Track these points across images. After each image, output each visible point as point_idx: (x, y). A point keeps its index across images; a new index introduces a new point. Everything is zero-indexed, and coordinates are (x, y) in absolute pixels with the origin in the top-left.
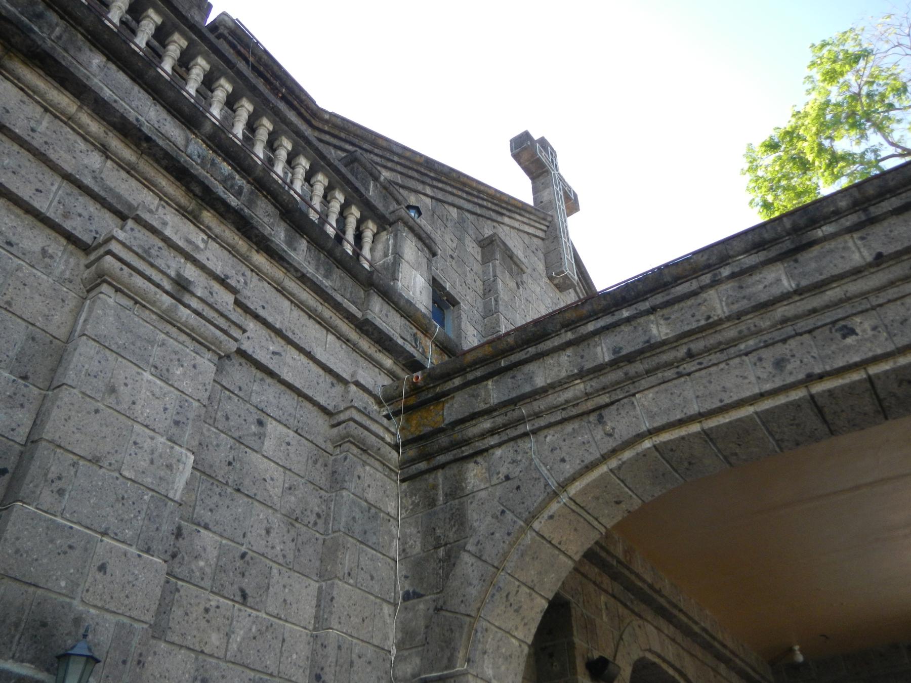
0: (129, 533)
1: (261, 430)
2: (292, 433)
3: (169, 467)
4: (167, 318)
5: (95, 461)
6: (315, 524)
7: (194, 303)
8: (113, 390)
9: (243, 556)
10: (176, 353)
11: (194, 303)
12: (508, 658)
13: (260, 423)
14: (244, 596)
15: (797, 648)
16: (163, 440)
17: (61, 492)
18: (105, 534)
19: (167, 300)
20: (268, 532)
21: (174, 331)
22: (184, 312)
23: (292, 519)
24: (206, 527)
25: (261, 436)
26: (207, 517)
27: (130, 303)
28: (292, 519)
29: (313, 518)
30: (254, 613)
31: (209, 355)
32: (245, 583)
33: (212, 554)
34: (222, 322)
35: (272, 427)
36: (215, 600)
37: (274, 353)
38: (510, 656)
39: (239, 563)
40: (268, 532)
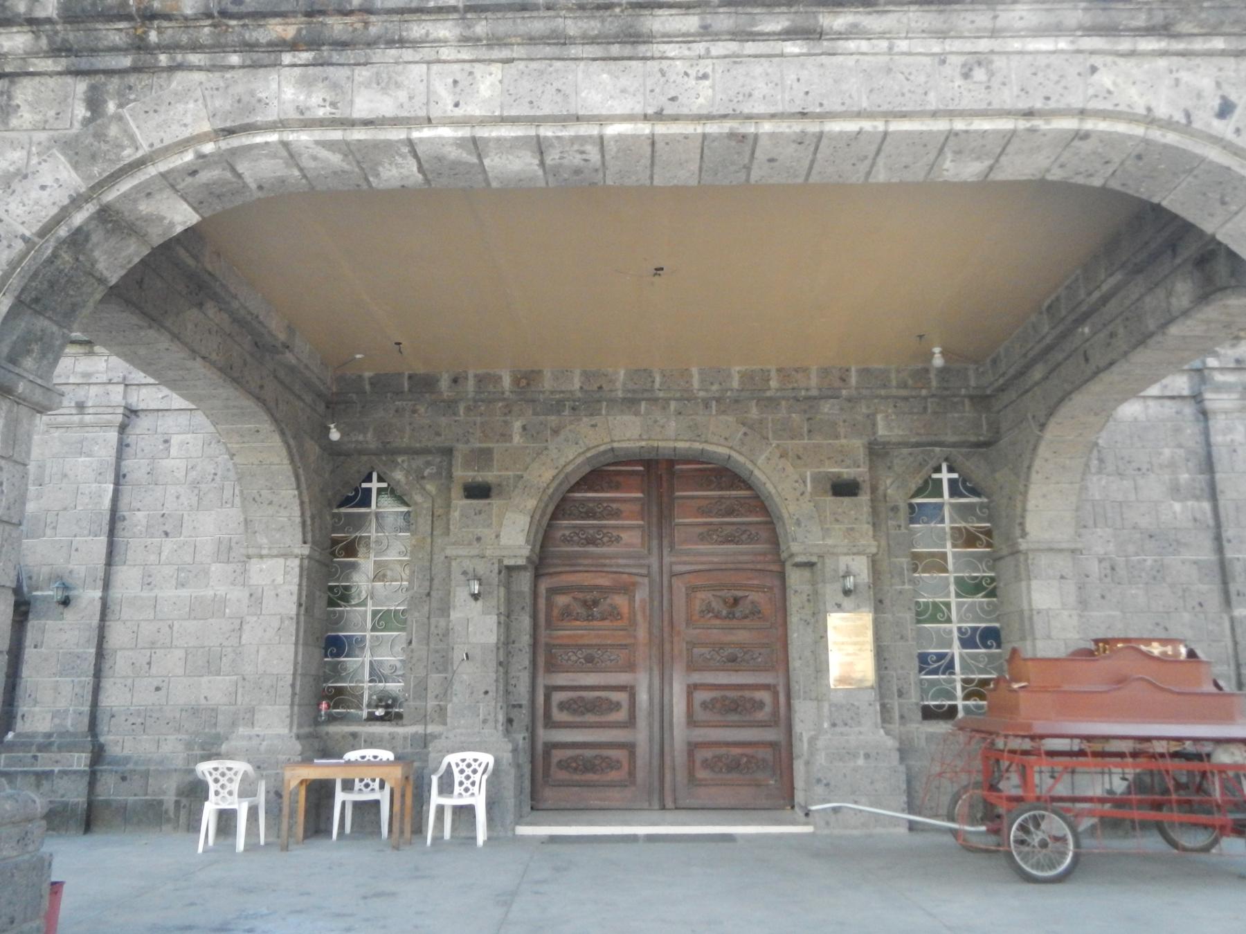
0: (86, 532)
1: (167, 445)
2: (189, 436)
3: (100, 496)
4: (83, 425)
5: (65, 509)
6: (213, 480)
7: (91, 411)
8: (65, 476)
9: (163, 515)
10: (93, 439)
11: (91, 411)
12: (281, 529)
13: (166, 441)
14: (166, 534)
15: (937, 350)
16: (94, 485)
17: (55, 528)
18: (75, 536)
19: (76, 418)
20: (178, 498)
21: (90, 429)
22: (87, 418)
23: (195, 485)
24: (139, 510)
25: (168, 449)
26: (139, 505)
27: (63, 430)
28: (195, 485)
29: (211, 477)
30: (174, 539)
31: (113, 429)
32: (166, 528)
33: (144, 522)
34: (110, 410)
35: (175, 440)
36: (149, 541)
37: (163, 398)
38: (283, 527)
39: (161, 520)
40: (178, 498)
